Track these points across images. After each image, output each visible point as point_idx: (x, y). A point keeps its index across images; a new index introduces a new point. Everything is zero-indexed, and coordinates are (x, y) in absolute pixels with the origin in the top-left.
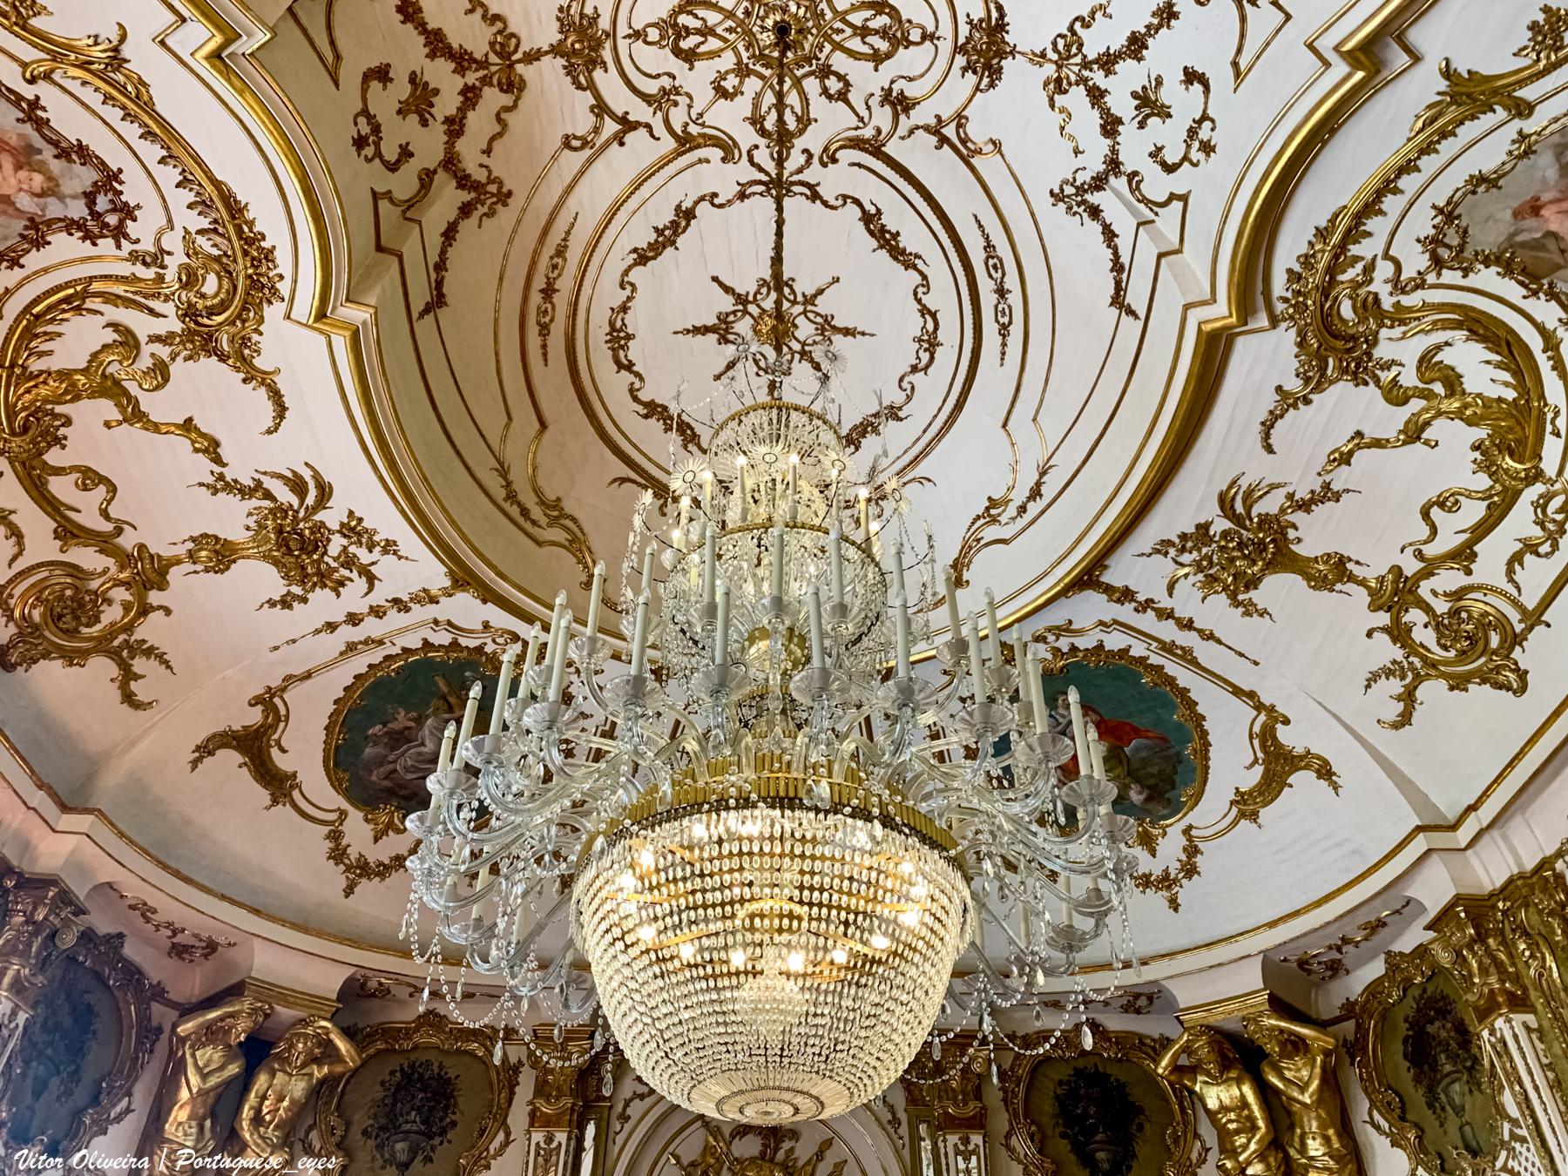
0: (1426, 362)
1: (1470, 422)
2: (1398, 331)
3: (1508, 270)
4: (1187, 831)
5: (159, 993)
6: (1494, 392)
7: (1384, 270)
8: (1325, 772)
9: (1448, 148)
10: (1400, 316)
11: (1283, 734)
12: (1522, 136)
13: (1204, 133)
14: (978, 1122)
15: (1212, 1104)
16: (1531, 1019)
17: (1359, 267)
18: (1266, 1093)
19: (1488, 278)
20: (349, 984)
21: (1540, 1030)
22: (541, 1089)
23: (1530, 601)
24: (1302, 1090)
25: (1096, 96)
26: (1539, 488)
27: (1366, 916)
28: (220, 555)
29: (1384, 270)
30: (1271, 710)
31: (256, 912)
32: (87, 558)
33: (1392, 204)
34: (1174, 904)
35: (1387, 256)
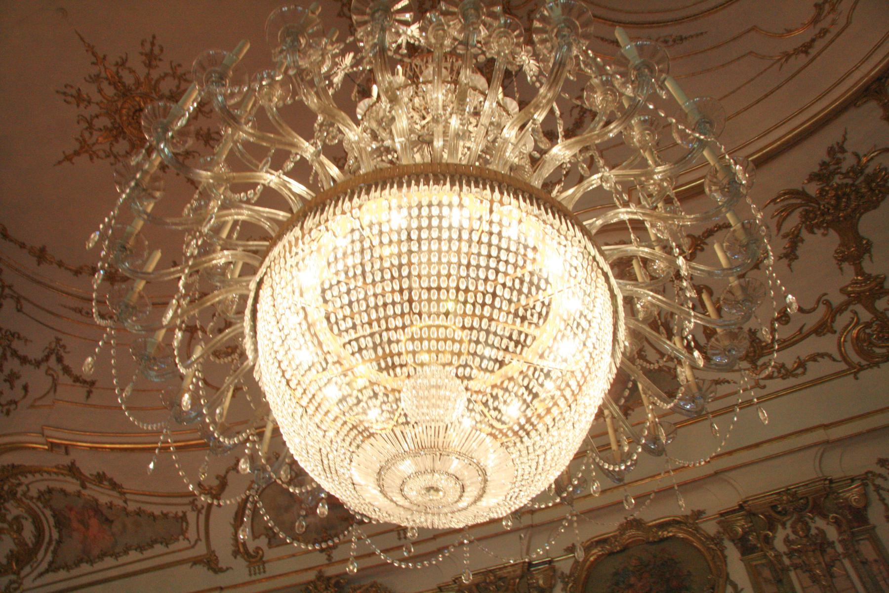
0: (17, 518)
1: (16, 544)
2: (15, 504)
3: (54, 516)
6: (29, 541)
7: (24, 488)
9: (61, 477)
10: (19, 502)
12: (79, 492)
13: (13, 406)
17: (17, 482)
19: (48, 513)
29: (24, 488)
33: (38, 476)
35: (27, 486)
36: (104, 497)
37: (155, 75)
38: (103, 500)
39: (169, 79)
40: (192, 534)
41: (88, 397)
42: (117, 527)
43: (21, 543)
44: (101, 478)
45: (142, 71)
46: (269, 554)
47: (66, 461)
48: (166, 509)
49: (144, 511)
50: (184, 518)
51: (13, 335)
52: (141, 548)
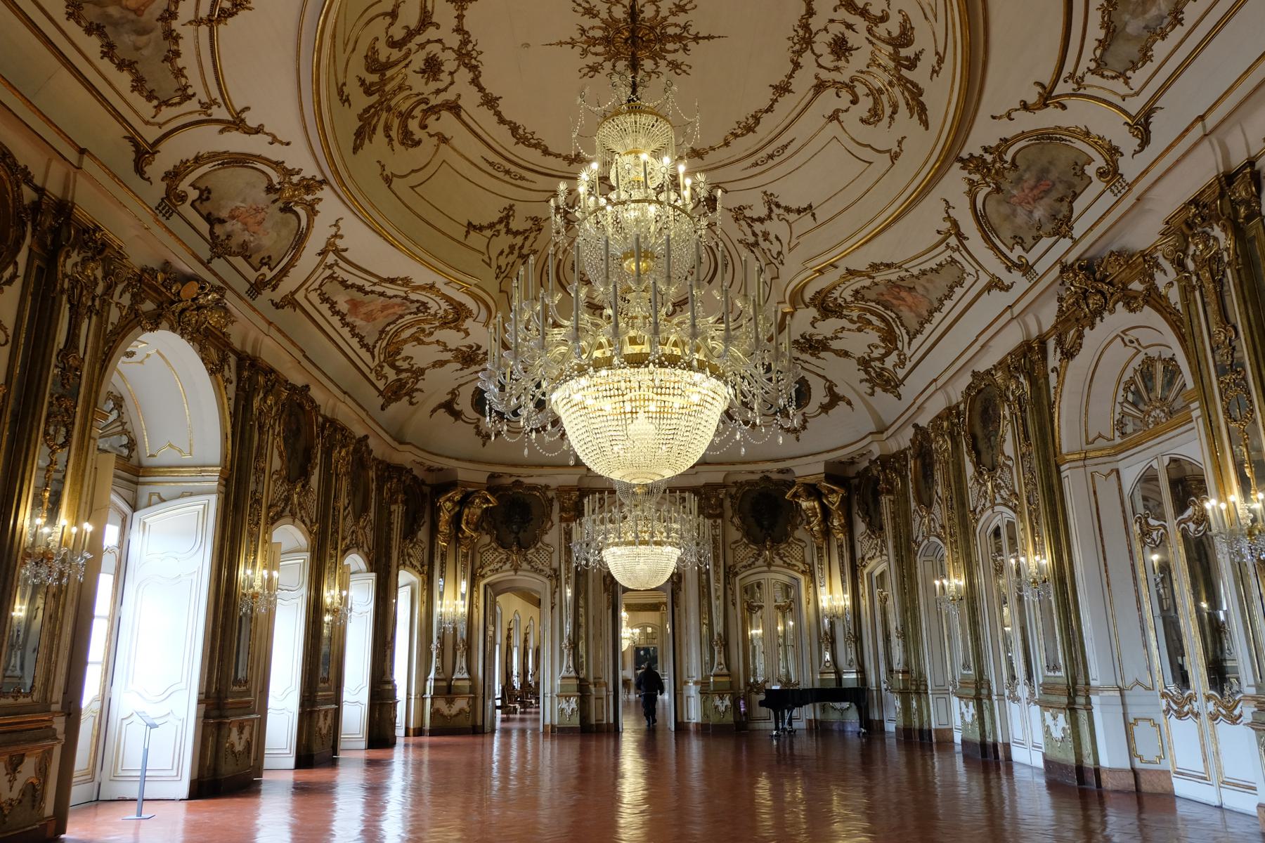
0: (859, 317)
3: (878, 304)
4: (804, 414)
5: (423, 482)
8: (849, 403)
9: (852, 281)
11: (835, 388)
14: (721, 516)
15: (804, 507)
16: (892, 497)
18: (823, 506)
19: (873, 304)
20: (489, 477)
21: (894, 502)
22: (562, 509)
23: (901, 376)
24: (833, 505)
25: (750, 226)
26: (896, 352)
27: (860, 452)
28: (442, 363)
30: (831, 382)
31: (457, 459)
32: (403, 375)
33: (840, 289)
34: (798, 439)
36: (893, 276)
37: (604, 15)
38: (894, 277)
39: (614, 8)
40: (968, 269)
41: (815, 219)
42: (920, 289)
43: (879, 330)
44: (875, 267)
45: (597, 22)
46: (1031, 257)
47: (842, 271)
48: (938, 260)
49: (925, 270)
50: (953, 261)
51: (739, 209)
52: (948, 297)
